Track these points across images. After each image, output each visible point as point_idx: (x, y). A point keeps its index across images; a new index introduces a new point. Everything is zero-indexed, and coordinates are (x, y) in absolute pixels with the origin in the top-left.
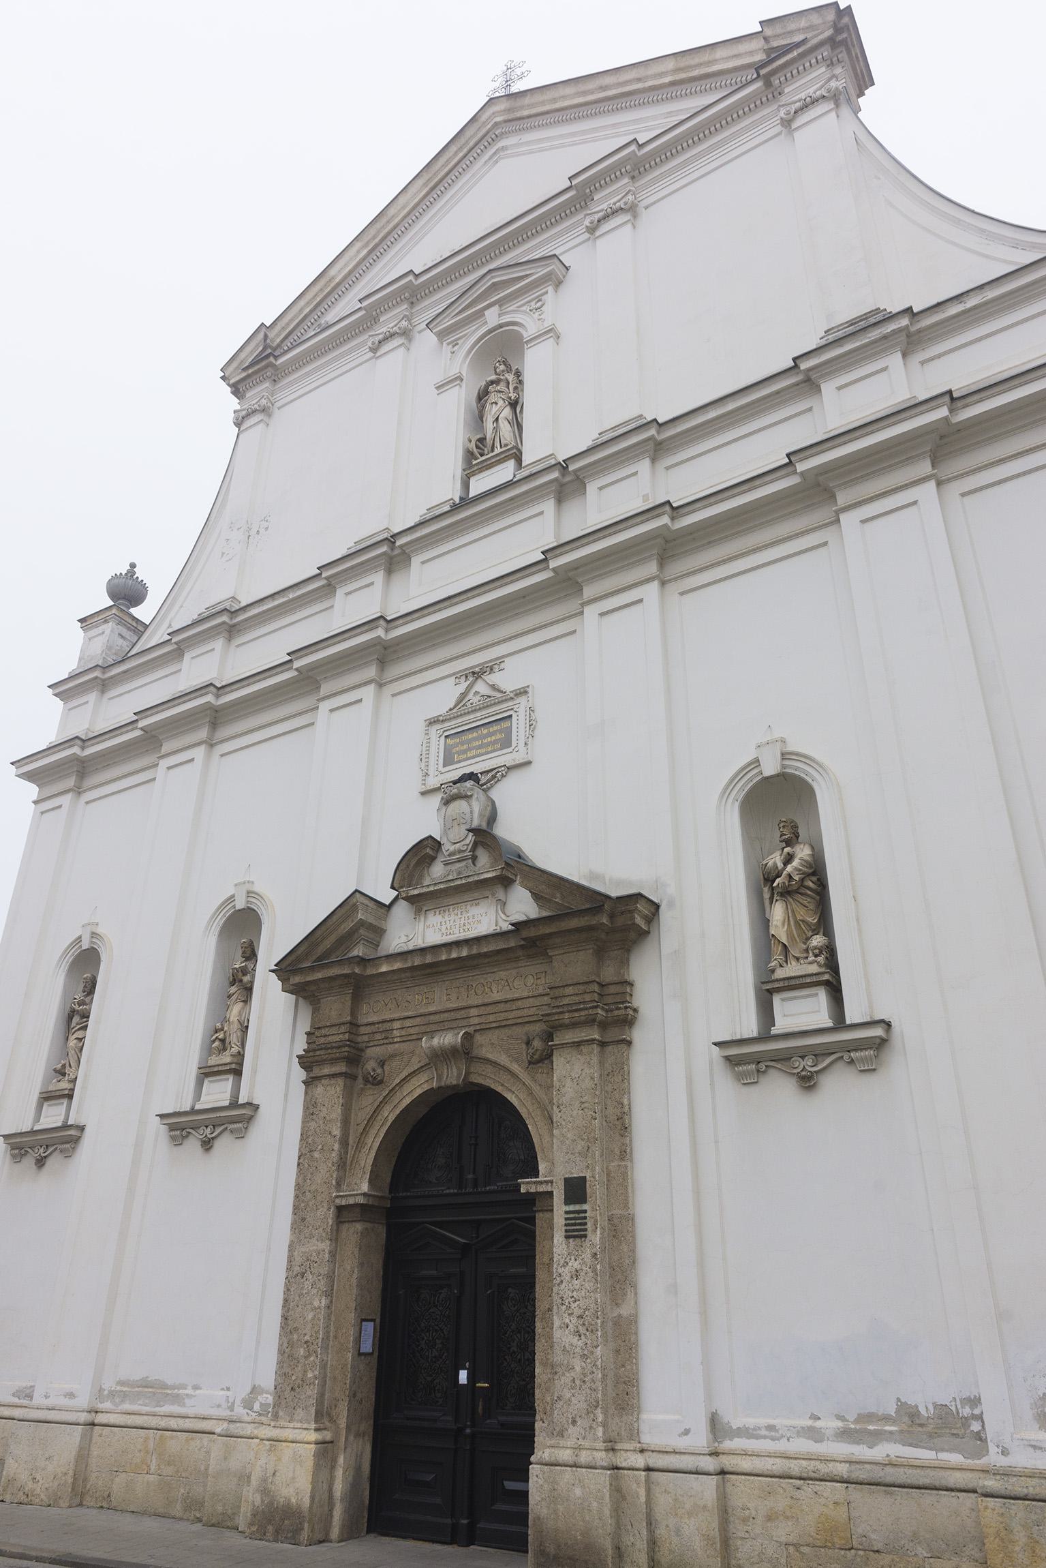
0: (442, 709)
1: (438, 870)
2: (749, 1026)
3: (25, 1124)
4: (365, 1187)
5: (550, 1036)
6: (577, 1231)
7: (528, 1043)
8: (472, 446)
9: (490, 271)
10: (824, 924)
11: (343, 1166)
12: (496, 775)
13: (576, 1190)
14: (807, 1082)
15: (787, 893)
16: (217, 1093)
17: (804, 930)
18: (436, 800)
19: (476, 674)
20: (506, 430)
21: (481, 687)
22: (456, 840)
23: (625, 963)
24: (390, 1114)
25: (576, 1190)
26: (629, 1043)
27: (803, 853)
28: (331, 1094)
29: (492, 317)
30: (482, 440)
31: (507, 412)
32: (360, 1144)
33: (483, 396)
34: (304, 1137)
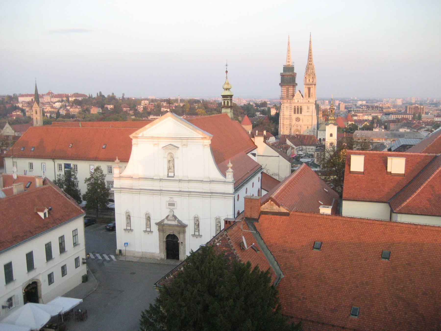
0: (168, 200)
1: (169, 217)
2: (193, 234)
3: (126, 228)
4: (165, 240)
5: (180, 233)
6: (182, 245)
7: (178, 232)
8: (168, 168)
9: (170, 144)
10: (199, 227)
11: (163, 238)
12: (174, 209)
13: (182, 243)
14: (197, 238)
15: (196, 225)
16: (148, 229)
17: (197, 228)
18: (169, 210)
19: (171, 198)
20: (172, 168)
21: (171, 199)
22: (171, 215)
23: (185, 229)
24: (167, 235)
25: (182, 243)
26: (185, 234)
27: (198, 222)
28: (162, 234)
29: (170, 151)
30: (170, 167)
31: (172, 165)
32: (164, 237)
33: (170, 161)
34: (159, 236)
